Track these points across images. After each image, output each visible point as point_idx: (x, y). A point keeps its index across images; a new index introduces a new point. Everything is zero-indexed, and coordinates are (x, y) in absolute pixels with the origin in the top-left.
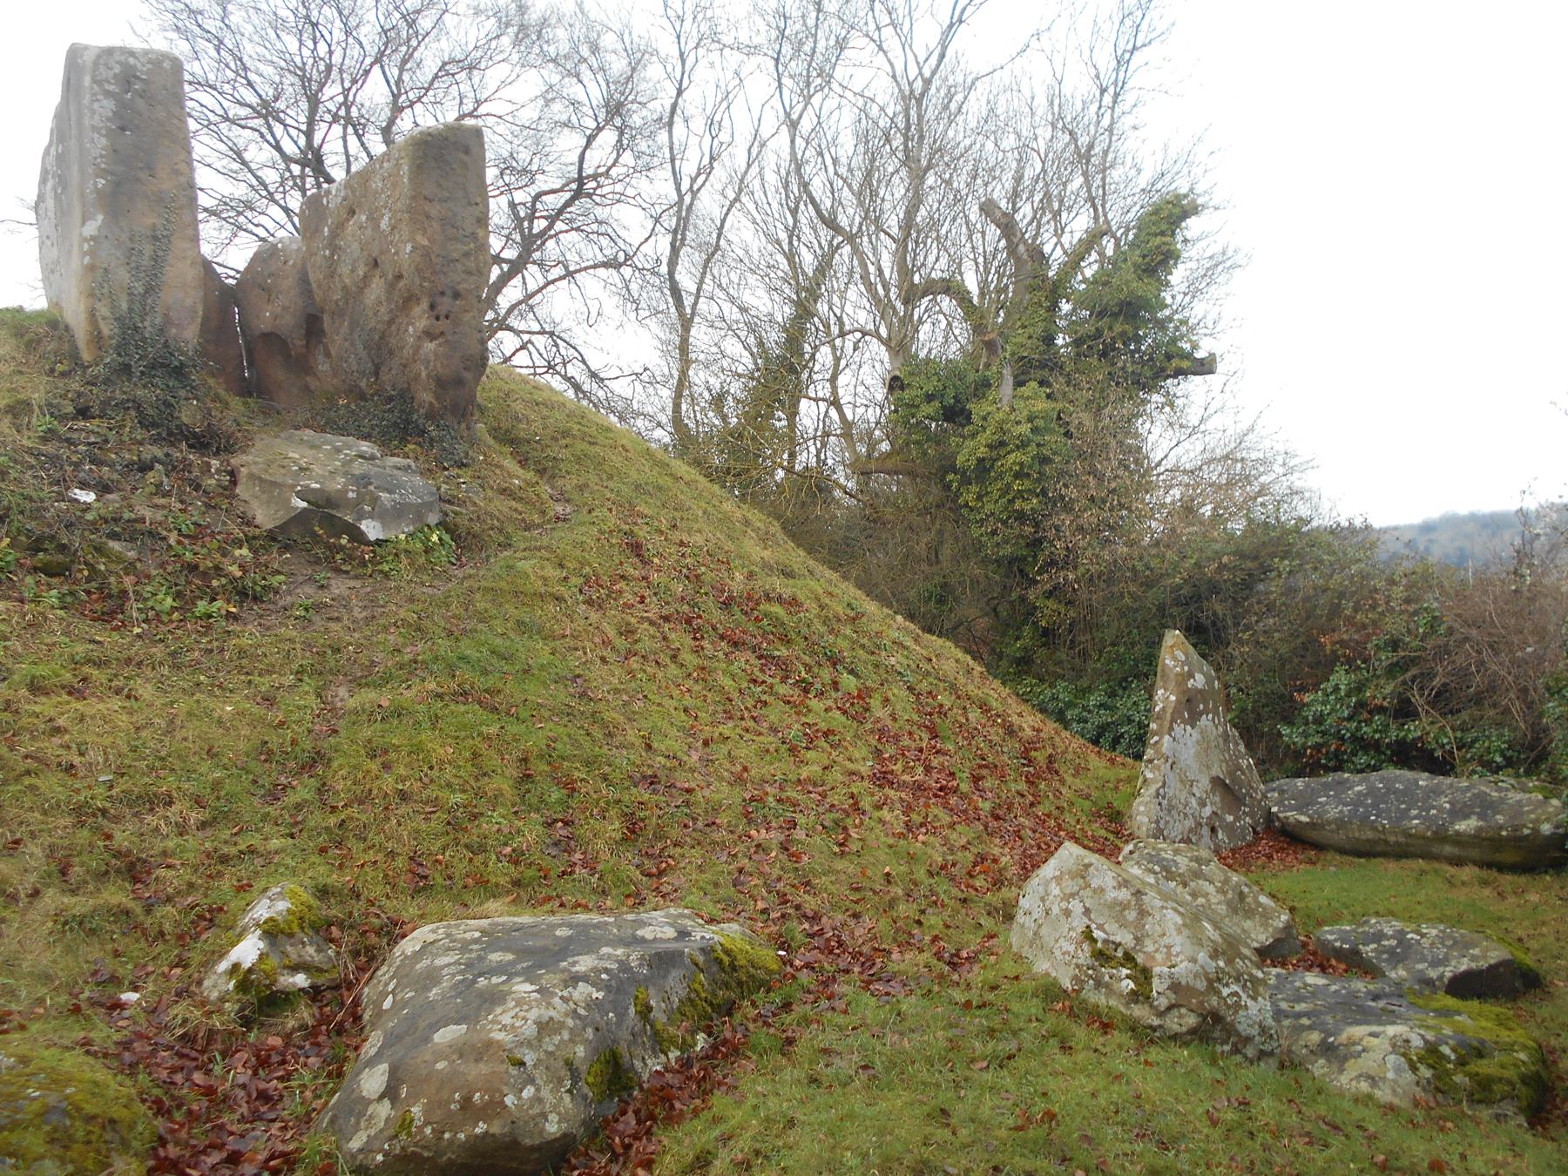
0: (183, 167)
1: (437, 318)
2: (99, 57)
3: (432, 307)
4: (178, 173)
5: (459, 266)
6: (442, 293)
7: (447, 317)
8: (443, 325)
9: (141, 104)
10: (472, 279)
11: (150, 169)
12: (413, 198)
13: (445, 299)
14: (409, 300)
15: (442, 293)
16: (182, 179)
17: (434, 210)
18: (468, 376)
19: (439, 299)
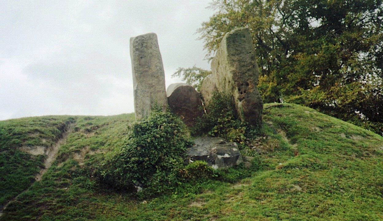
0: (158, 64)
1: (242, 93)
2: (135, 39)
3: (239, 90)
4: (157, 66)
5: (247, 74)
6: (242, 85)
7: (245, 92)
8: (243, 95)
9: (145, 49)
10: (252, 78)
11: (149, 67)
12: (228, 56)
13: (243, 86)
14: (233, 88)
15: (242, 85)
16: (158, 68)
17: (236, 58)
18: (256, 110)
19: (241, 87)
